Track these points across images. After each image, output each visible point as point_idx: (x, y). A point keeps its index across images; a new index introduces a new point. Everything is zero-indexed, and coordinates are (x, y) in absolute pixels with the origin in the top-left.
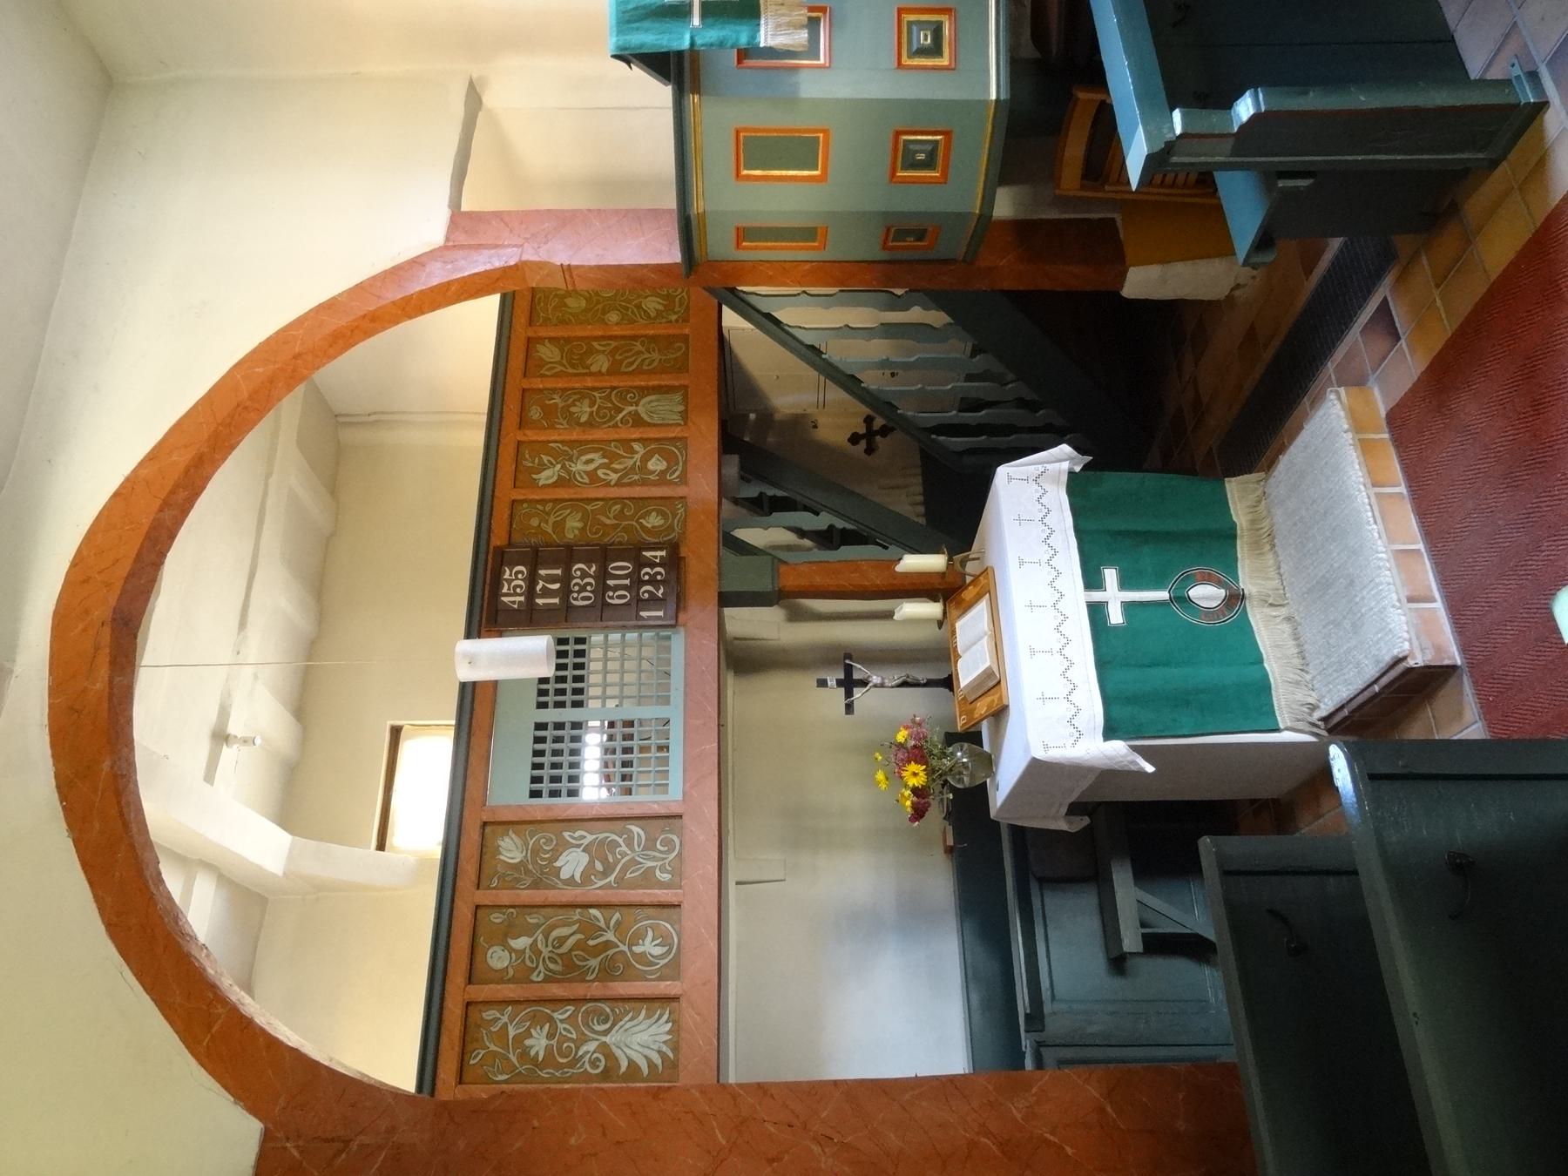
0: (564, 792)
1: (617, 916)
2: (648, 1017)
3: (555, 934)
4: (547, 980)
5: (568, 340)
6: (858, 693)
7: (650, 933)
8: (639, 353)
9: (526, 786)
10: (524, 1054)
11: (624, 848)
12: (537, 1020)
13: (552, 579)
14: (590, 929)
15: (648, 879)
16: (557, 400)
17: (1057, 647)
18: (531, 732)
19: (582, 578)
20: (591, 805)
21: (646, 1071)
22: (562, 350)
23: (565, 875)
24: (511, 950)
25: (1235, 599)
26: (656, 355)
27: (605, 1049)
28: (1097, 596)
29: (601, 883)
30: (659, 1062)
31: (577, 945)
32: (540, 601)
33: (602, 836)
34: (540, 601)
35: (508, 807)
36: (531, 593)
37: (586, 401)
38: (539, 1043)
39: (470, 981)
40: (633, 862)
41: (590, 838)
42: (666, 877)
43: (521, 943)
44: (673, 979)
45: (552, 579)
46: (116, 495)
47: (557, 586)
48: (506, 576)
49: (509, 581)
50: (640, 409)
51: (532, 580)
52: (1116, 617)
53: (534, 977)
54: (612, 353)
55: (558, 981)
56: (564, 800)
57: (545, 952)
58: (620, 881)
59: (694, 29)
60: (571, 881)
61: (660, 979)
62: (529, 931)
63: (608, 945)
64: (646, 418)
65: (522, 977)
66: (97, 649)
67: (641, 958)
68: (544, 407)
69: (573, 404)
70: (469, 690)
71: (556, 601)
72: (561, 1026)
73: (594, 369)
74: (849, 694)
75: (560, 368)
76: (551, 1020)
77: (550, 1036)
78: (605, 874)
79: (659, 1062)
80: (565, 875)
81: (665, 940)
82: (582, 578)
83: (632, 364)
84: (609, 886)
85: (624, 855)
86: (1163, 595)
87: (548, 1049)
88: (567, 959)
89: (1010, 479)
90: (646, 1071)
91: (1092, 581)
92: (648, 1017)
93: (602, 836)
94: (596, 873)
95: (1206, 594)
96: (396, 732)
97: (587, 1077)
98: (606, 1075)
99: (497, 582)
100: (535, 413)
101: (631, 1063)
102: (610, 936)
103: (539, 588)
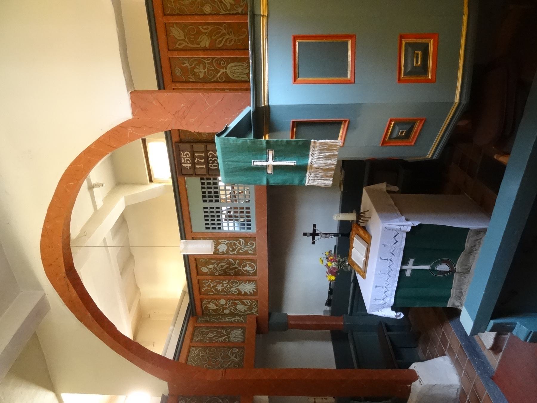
0: (217, 228)
1: (238, 261)
2: (249, 283)
3: (220, 265)
4: (219, 275)
5: (186, 25)
6: (317, 237)
7: (248, 266)
8: (224, 34)
9: (205, 226)
10: (216, 290)
11: (238, 245)
12: (220, 283)
13: (201, 158)
14: (230, 264)
15: (246, 253)
16: (187, 64)
17: (385, 285)
18: (203, 210)
19: (213, 157)
20: (226, 233)
21: (249, 294)
22: (184, 32)
23: (221, 250)
24: (208, 268)
25: (452, 271)
26: (232, 37)
27: (237, 289)
28: (404, 267)
29: (232, 253)
30: (252, 292)
31: (227, 268)
32: (197, 166)
33: (231, 241)
34: (197, 166)
35: (199, 233)
36: (193, 163)
37: (201, 65)
38: (219, 287)
39: (198, 274)
40: (241, 248)
41: (227, 242)
42: (252, 252)
43: (211, 266)
44: (254, 276)
45: (201, 158)
46: (43, 236)
47: (203, 161)
48: (182, 156)
49: (184, 158)
50: (227, 71)
51: (193, 157)
52: (408, 274)
53: (216, 274)
54: (210, 34)
55: (223, 275)
56: (217, 231)
57: (218, 269)
58: (238, 253)
59: (269, 175)
60: (223, 252)
61: (252, 275)
62: (213, 264)
63: (236, 268)
64: (230, 76)
65: (212, 274)
66: (68, 285)
67: (246, 271)
68: (182, 69)
69: (195, 67)
70: (169, 133)
71: (204, 166)
72: (225, 285)
73: (202, 45)
74: (314, 230)
75: (185, 44)
76: (223, 283)
77: (223, 286)
78: (234, 250)
79: (252, 292)
80: (221, 250)
81: (253, 267)
82: (213, 157)
83: (221, 42)
84: (234, 254)
85: (238, 246)
86: (428, 268)
87: (223, 289)
88: (225, 271)
89: (386, 229)
90: (249, 294)
91: (405, 262)
92: (249, 283)
93: (231, 241)
94: (230, 251)
95: (443, 267)
96: (144, 141)
97: (233, 294)
98: (238, 294)
99: (179, 159)
100: (178, 72)
101: (245, 293)
102: (236, 266)
103: (196, 161)
